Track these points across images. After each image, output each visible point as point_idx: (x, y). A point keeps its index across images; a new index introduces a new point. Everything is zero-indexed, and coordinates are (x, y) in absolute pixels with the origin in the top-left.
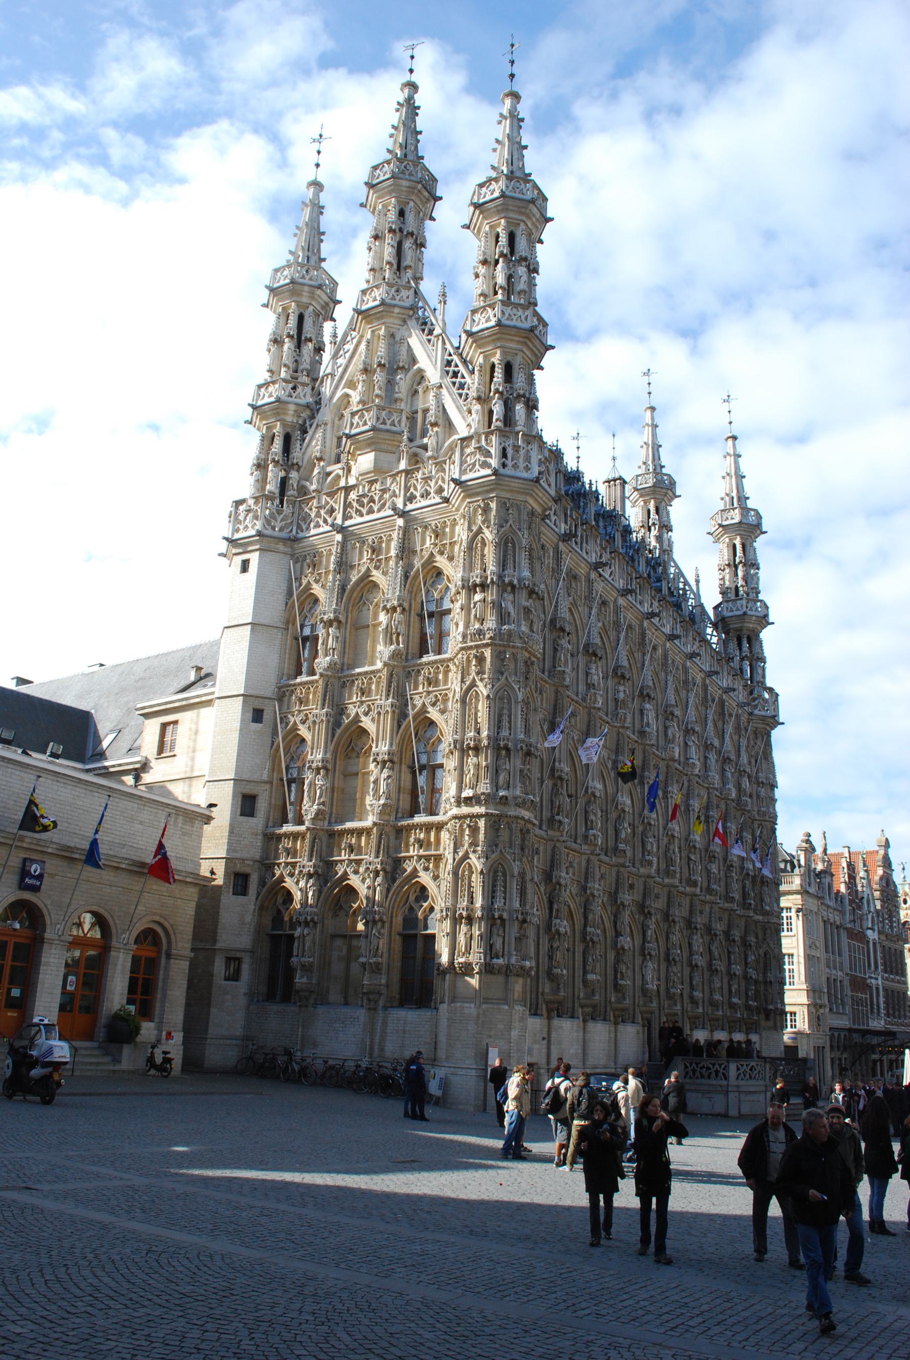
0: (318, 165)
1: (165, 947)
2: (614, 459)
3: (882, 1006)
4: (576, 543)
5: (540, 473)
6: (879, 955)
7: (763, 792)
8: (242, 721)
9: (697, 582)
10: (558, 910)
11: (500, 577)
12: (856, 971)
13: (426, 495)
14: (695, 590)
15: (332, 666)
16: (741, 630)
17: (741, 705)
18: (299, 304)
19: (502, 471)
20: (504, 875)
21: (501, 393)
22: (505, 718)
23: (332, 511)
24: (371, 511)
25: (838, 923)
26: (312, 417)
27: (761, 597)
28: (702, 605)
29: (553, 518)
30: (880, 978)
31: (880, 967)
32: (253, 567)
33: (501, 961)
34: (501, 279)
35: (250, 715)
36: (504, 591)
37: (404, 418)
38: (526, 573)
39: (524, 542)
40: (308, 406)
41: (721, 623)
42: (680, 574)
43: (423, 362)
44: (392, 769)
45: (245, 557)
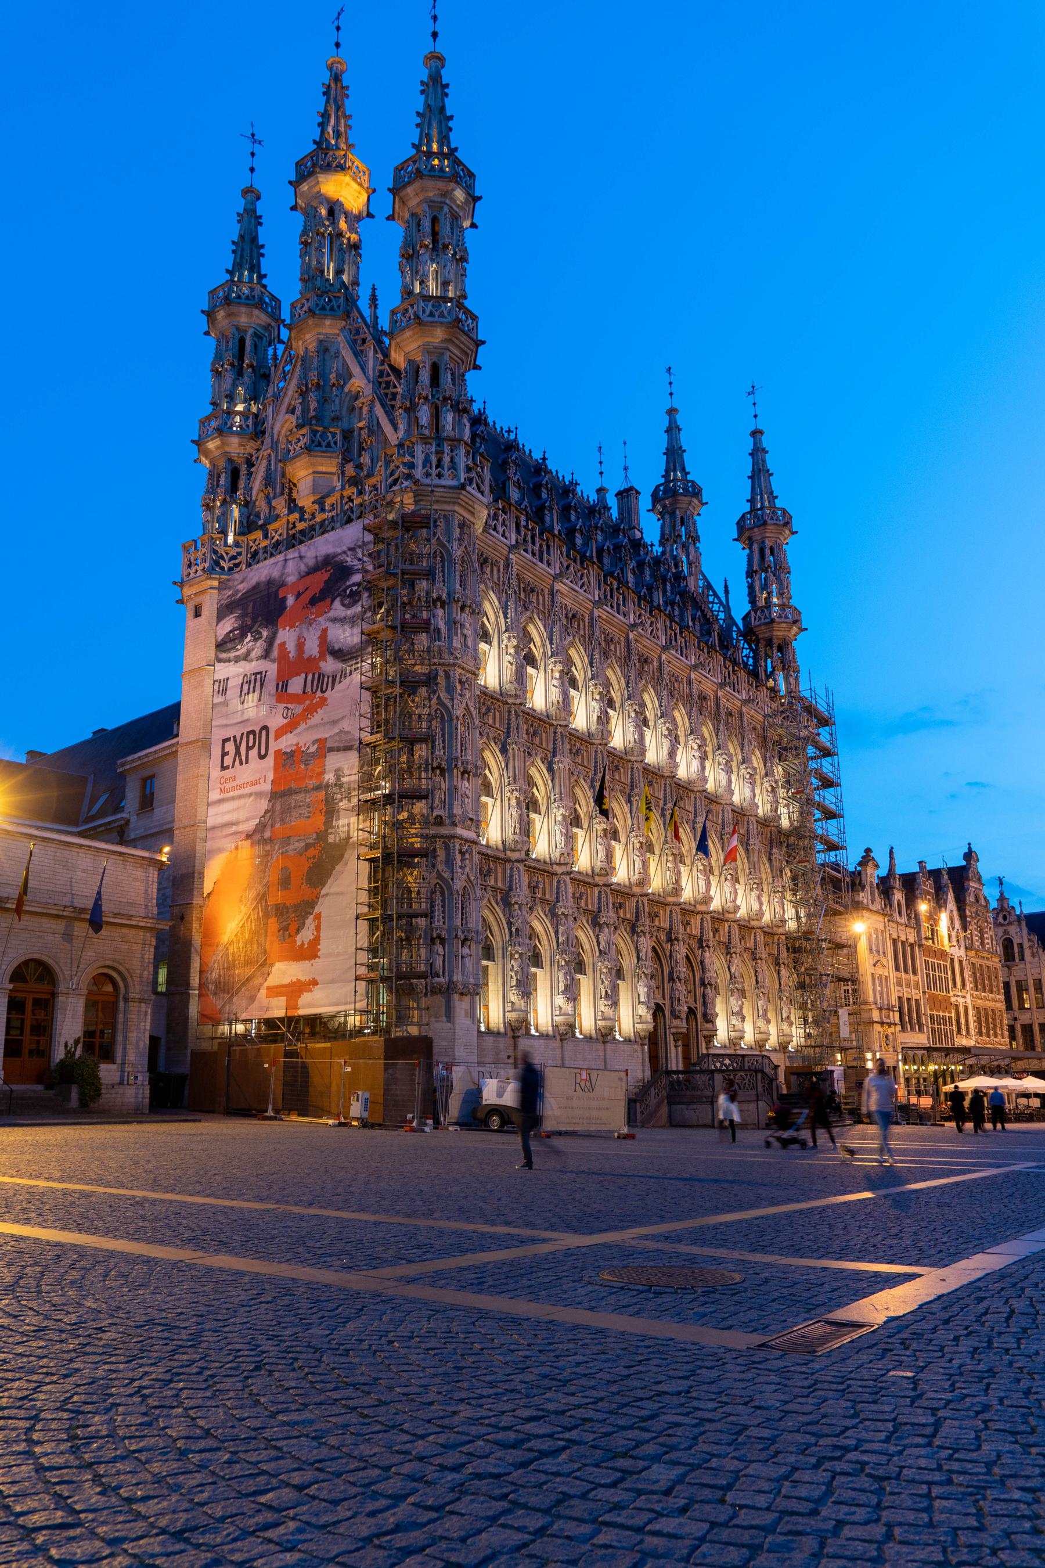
1: (122, 990)
2: (626, 469)
3: (972, 1025)
4: (534, 554)
6: (967, 974)
9: (727, 591)
10: (517, 930)
12: (935, 989)
14: (724, 600)
25: (912, 940)
27: (792, 602)
29: (501, 529)
30: (968, 996)
31: (969, 986)
33: (441, 980)
41: (749, 633)
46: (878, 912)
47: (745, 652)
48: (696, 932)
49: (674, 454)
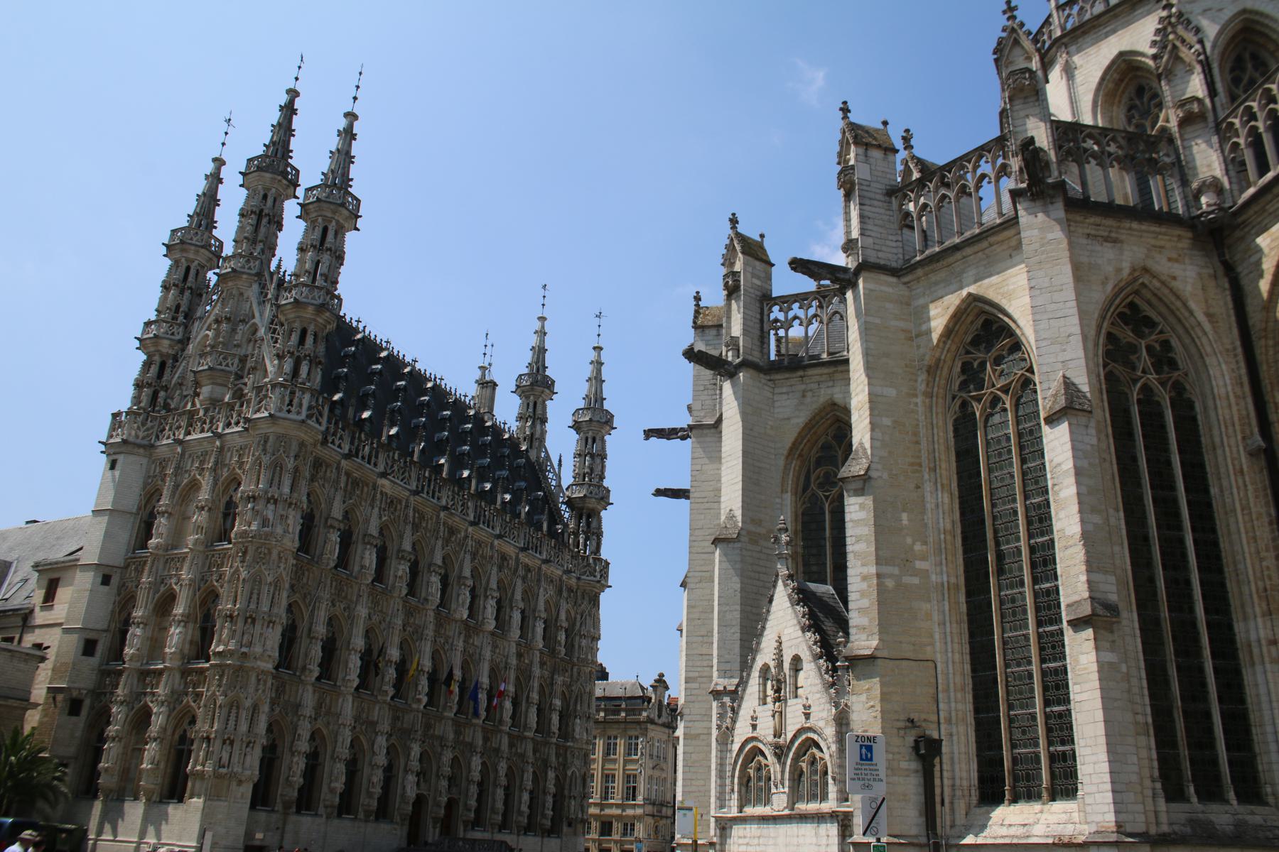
0: (223, 144)
4: (363, 458)
5: (309, 417)
7: (584, 642)
8: (93, 584)
11: (266, 492)
13: (237, 423)
15: (157, 547)
16: (582, 509)
17: (568, 572)
18: (187, 259)
19: (278, 414)
20: (238, 708)
21: (292, 354)
22: (255, 596)
23: (179, 428)
24: (202, 431)
26: (183, 350)
28: (559, 485)
29: (337, 443)
32: (118, 466)
34: (307, 266)
35: (100, 580)
36: (268, 502)
37: (236, 361)
38: (286, 490)
39: (289, 466)
40: (180, 341)
42: (548, 457)
43: (257, 320)
44: (185, 626)
45: (115, 457)
46: (664, 725)
47: (567, 515)
48: (468, 739)
49: (540, 352)
